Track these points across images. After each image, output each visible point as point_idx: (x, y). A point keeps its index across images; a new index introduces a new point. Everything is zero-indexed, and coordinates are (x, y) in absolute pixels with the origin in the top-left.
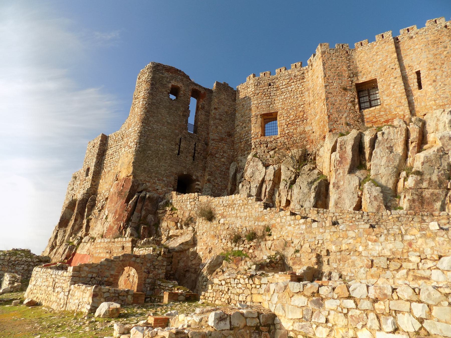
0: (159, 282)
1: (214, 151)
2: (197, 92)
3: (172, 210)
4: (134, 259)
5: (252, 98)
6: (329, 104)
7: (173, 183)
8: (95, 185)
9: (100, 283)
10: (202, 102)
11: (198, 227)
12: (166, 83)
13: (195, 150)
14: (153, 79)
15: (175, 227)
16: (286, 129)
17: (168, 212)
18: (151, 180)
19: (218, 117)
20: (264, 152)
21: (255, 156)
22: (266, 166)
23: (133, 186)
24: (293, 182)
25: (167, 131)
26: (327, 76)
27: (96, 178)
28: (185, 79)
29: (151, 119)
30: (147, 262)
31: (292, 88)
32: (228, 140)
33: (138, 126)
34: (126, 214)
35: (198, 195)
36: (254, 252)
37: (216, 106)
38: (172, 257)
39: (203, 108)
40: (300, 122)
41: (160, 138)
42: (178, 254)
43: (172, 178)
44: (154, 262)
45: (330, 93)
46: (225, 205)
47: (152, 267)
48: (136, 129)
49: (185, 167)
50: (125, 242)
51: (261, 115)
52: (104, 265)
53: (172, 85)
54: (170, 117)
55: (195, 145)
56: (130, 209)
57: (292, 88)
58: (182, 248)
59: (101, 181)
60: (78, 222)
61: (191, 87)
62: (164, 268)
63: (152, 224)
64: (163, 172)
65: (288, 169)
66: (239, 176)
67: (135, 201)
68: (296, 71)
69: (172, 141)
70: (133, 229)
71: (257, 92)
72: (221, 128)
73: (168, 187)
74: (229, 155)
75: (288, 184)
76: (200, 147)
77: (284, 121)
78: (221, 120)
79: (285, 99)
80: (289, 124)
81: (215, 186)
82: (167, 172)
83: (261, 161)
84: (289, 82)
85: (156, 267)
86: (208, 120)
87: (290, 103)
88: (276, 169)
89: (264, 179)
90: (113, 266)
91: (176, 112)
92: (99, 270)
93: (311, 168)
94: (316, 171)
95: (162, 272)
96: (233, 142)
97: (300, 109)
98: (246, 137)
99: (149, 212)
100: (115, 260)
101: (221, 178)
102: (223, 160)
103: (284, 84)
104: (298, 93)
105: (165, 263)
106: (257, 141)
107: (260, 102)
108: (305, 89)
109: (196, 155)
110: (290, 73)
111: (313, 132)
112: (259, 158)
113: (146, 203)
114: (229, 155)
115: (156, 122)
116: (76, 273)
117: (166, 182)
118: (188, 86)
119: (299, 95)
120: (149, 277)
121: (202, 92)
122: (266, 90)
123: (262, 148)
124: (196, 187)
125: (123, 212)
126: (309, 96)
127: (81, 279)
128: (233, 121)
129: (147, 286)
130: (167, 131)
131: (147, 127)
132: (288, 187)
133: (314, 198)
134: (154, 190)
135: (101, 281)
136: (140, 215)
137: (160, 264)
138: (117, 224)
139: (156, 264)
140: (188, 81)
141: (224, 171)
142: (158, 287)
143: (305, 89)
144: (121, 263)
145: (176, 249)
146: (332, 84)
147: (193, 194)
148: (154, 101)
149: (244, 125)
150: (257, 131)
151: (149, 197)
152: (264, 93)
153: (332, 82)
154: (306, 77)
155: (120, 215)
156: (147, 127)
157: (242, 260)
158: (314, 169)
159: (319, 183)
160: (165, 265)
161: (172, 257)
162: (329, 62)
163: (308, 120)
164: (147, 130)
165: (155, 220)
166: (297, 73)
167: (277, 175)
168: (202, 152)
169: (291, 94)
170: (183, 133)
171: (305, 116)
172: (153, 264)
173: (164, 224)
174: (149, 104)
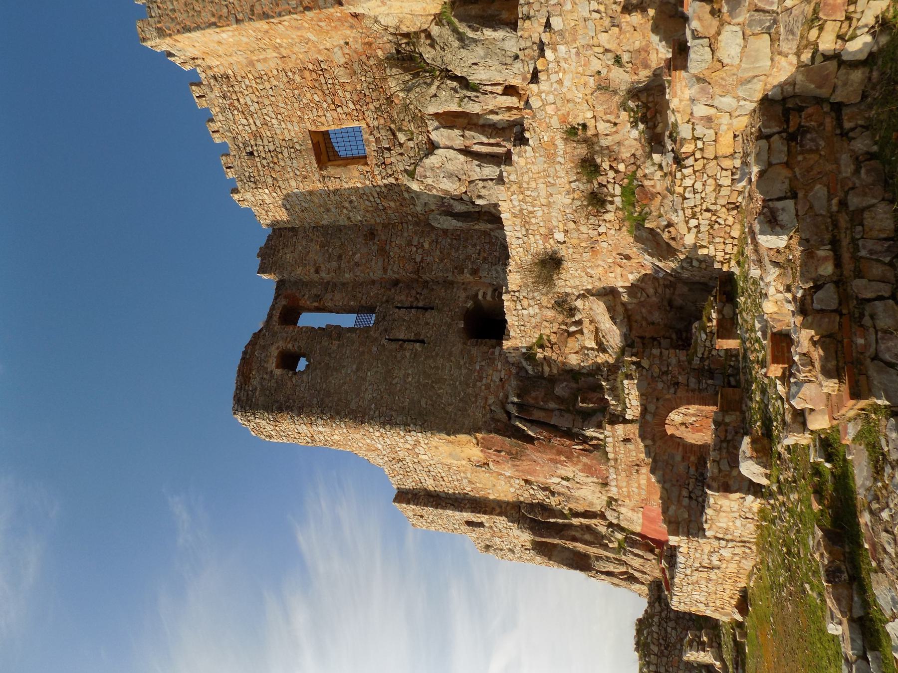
0: (696, 361)
1: (410, 267)
2: (287, 313)
3: (542, 346)
4: (649, 417)
5: (285, 192)
6: (277, 10)
7: (485, 349)
8: (501, 507)
9: (700, 481)
10: (305, 301)
11: (574, 287)
12: (273, 381)
13: (411, 307)
14: (268, 408)
15: (578, 336)
16: (345, 109)
17: (548, 353)
18: (482, 394)
19: (334, 264)
20: (401, 154)
21: (411, 174)
22: (432, 147)
23: (498, 432)
24: (464, 82)
25: (375, 370)
26: (213, 20)
27: (486, 507)
28: (261, 342)
29: (353, 406)
30: (655, 390)
31: (253, 101)
32: (383, 238)
33: (371, 430)
34: (556, 441)
35: (508, 292)
36: (623, 161)
37: (312, 270)
38: (642, 338)
39: (318, 298)
40: (327, 76)
41: (391, 383)
42: (635, 324)
43: (474, 351)
44: (655, 375)
45: (252, 10)
46: (524, 233)
47: (665, 378)
48: (377, 434)
49: (449, 326)
50: (614, 438)
51: (321, 169)
52: (664, 475)
53: (277, 367)
54: (344, 367)
55: (399, 308)
56: (545, 433)
57: (253, 101)
58: (621, 317)
59: (491, 497)
60: (578, 535)
61: (277, 327)
62: (666, 352)
63: (574, 385)
64: (464, 371)
65: (435, 96)
66: (459, 208)
67: (529, 425)
68: (213, 96)
69: (396, 357)
70: (586, 423)
71: (270, 180)
72: (358, 256)
73: (494, 359)
74: (415, 233)
75: (469, 94)
76: (403, 297)
77: (328, 115)
78: (340, 257)
79: (279, 116)
80: (333, 103)
81: (485, 259)
82: (462, 362)
83: (421, 159)
84: (238, 110)
85: (664, 369)
86: (344, 284)
87: (287, 104)
88: (436, 124)
89: (460, 151)
90: (665, 458)
91: (333, 355)
92: (673, 485)
93: (428, 42)
94: (435, 30)
95: (675, 357)
96: (385, 226)
97: (298, 78)
98: (371, 199)
99: (550, 395)
100: (653, 455)
101: (466, 247)
102: (426, 246)
103: (245, 122)
104: (261, 87)
105: (656, 351)
106: (380, 174)
107: (291, 174)
108: (250, 72)
109: (421, 304)
110: (218, 109)
111: (347, 43)
112: (416, 165)
113: (532, 401)
114: (415, 233)
115: (358, 395)
116: (681, 530)
117: (483, 363)
118: (274, 334)
119: (266, 83)
120: (685, 382)
121: (284, 302)
122: (265, 162)
123: (393, 160)
124: (489, 298)
125: (553, 447)
126: (265, 60)
127: (693, 519)
128: (340, 229)
129: (705, 386)
130: (375, 370)
131: (372, 413)
132: (475, 94)
133: (495, 30)
134: (503, 388)
135: (696, 479)
136: (557, 413)
137: (657, 361)
138: (578, 457)
139: (657, 370)
140: (264, 335)
141: (452, 239)
142: (706, 363)
143: (250, 72)
144: (659, 443)
145: (625, 330)
146: (231, 6)
147: (506, 303)
148: (315, 402)
149: (347, 204)
150: (357, 174)
151: (518, 396)
152: (272, 165)
153: (226, 6)
154: (222, 70)
155: (560, 453)
156: (372, 413)
157: (642, 186)
158: (429, 36)
159: (460, 21)
160: (659, 350)
161: (642, 338)
162: (181, 17)
163: (320, 59)
164: (377, 412)
165: (565, 381)
166: (217, 92)
167: (449, 120)
168: (413, 292)
169: (267, 102)
170: (377, 335)
171: (311, 67)
172: (658, 377)
173: (574, 360)
174: (322, 412)
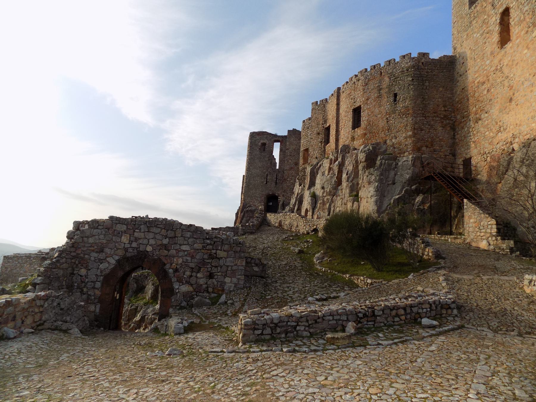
1: (286, 177)
78: (291, 156)
